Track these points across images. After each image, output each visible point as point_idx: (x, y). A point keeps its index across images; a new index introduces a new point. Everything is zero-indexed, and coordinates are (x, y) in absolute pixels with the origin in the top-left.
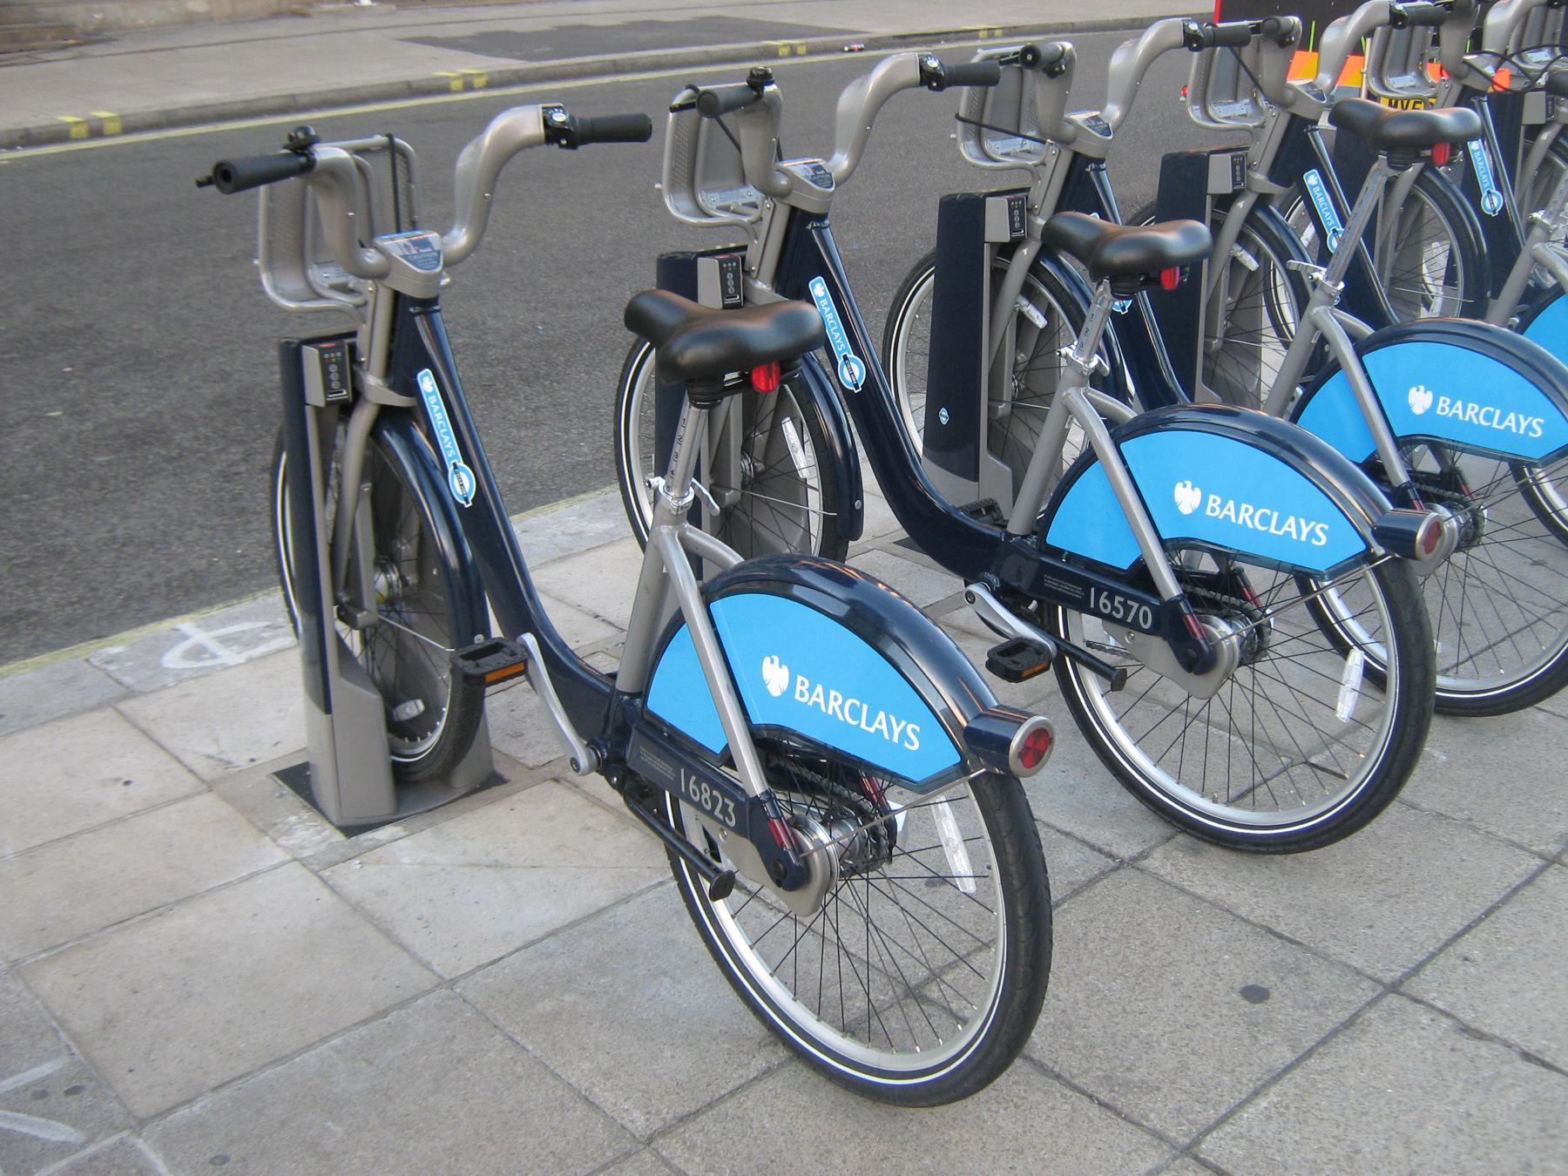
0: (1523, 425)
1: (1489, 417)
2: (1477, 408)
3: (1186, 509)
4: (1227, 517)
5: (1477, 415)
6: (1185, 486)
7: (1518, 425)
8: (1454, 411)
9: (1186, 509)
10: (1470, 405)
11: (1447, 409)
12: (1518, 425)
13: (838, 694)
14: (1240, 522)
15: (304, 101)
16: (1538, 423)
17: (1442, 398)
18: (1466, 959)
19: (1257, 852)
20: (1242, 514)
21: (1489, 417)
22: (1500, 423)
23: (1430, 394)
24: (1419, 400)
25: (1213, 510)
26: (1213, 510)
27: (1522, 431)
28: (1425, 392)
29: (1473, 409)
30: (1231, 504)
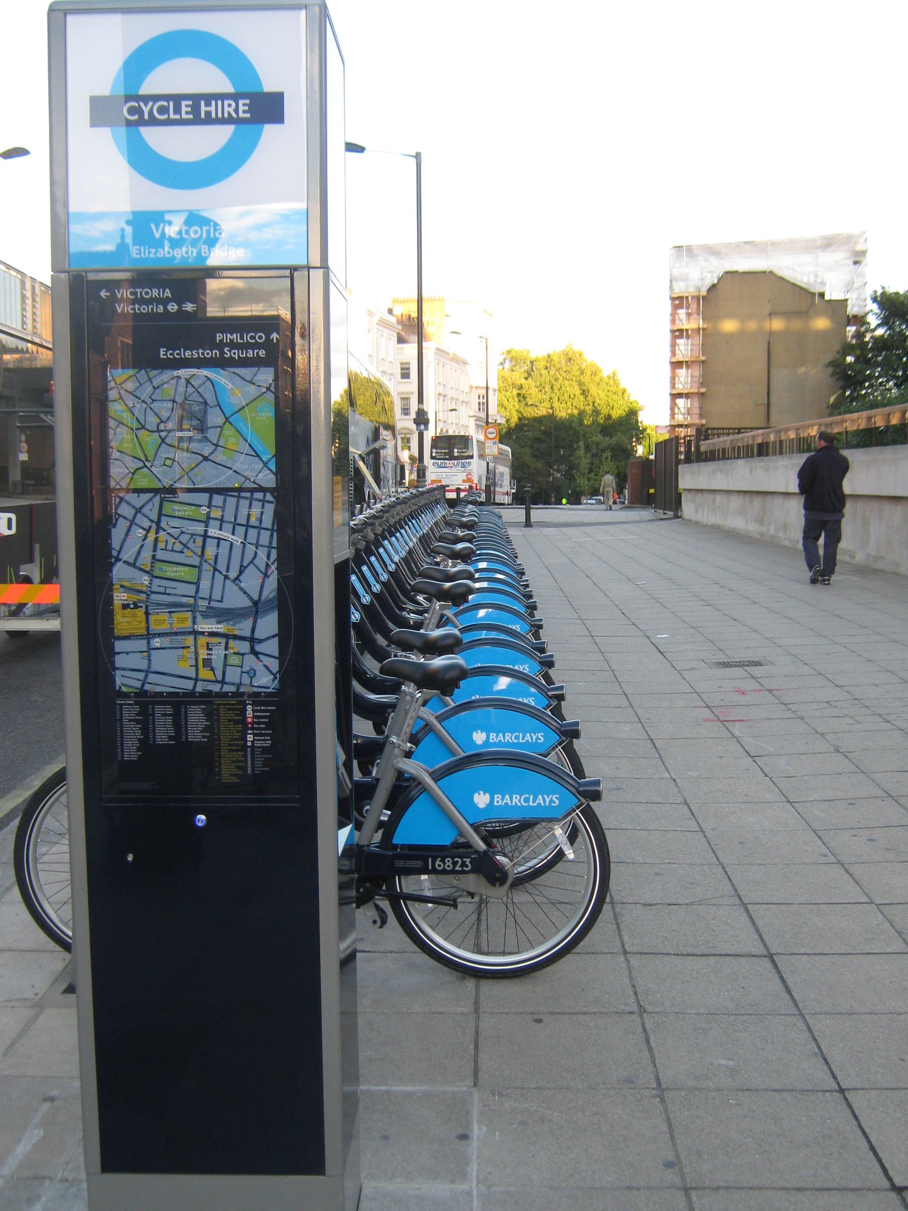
0: (548, 800)
1: (527, 800)
2: (518, 797)
3: (482, 805)
4: (506, 804)
5: (519, 801)
6: (479, 794)
7: (544, 801)
8: (505, 801)
9: (482, 805)
10: (514, 796)
11: (501, 801)
12: (544, 801)
13: (440, 869)
14: (514, 804)
15: (516, 526)
16: (556, 798)
17: (496, 796)
18: (755, 603)
19: (525, 974)
20: (514, 800)
21: (527, 800)
22: (534, 802)
23: (488, 795)
24: (481, 800)
25: (498, 802)
26: (498, 802)
27: (547, 804)
28: (484, 794)
29: (516, 798)
30: (507, 796)
